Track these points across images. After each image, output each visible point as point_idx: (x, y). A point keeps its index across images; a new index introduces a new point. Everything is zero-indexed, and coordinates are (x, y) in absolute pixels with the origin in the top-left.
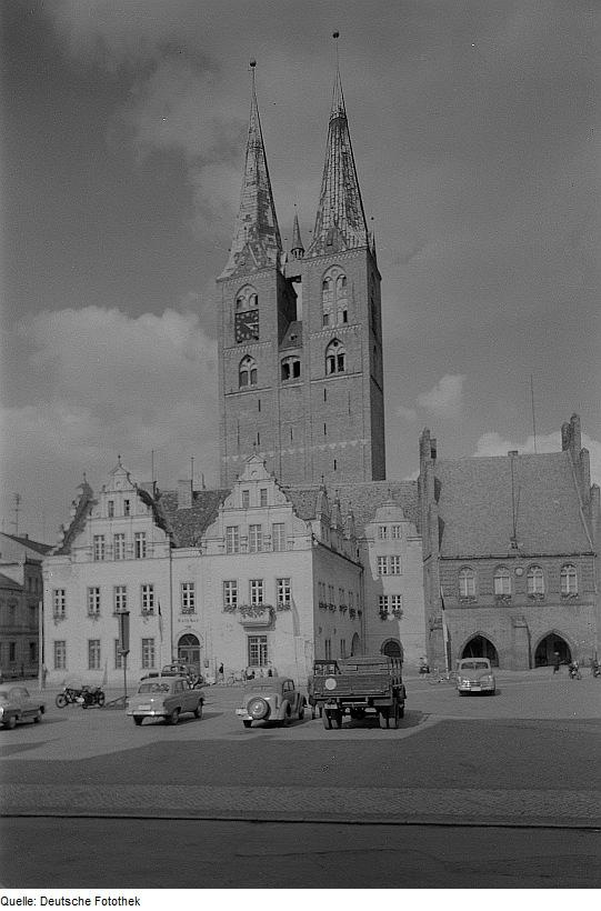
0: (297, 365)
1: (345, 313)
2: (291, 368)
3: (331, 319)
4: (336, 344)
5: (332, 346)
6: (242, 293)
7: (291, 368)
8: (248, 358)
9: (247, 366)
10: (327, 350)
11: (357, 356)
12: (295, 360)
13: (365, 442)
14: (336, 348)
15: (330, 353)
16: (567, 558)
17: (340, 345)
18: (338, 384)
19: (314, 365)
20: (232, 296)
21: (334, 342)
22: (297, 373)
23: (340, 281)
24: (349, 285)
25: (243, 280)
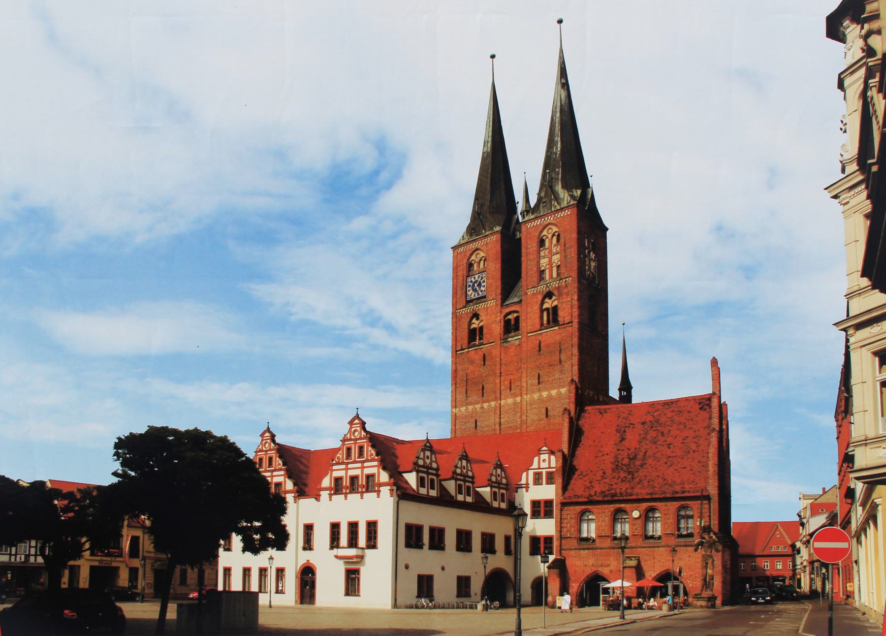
0: (517, 319)
1: (558, 267)
2: (513, 323)
3: (547, 276)
4: (550, 298)
5: (547, 300)
8: (476, 316)
9: (476, 324)
10: (542, 303)
11: (569, 308)
12: (515, 315)
13: (563, 390)
14: (550, 301)
15: (545, 306)
16: (702, 504)
17: (554, 298)
18: (552, 334)
19: (530, 318)
20: (465, 261)
21: (549, 295)
22: (517, 328)
23: (555, 239)
24: (562, 241)
25: (473, 246)
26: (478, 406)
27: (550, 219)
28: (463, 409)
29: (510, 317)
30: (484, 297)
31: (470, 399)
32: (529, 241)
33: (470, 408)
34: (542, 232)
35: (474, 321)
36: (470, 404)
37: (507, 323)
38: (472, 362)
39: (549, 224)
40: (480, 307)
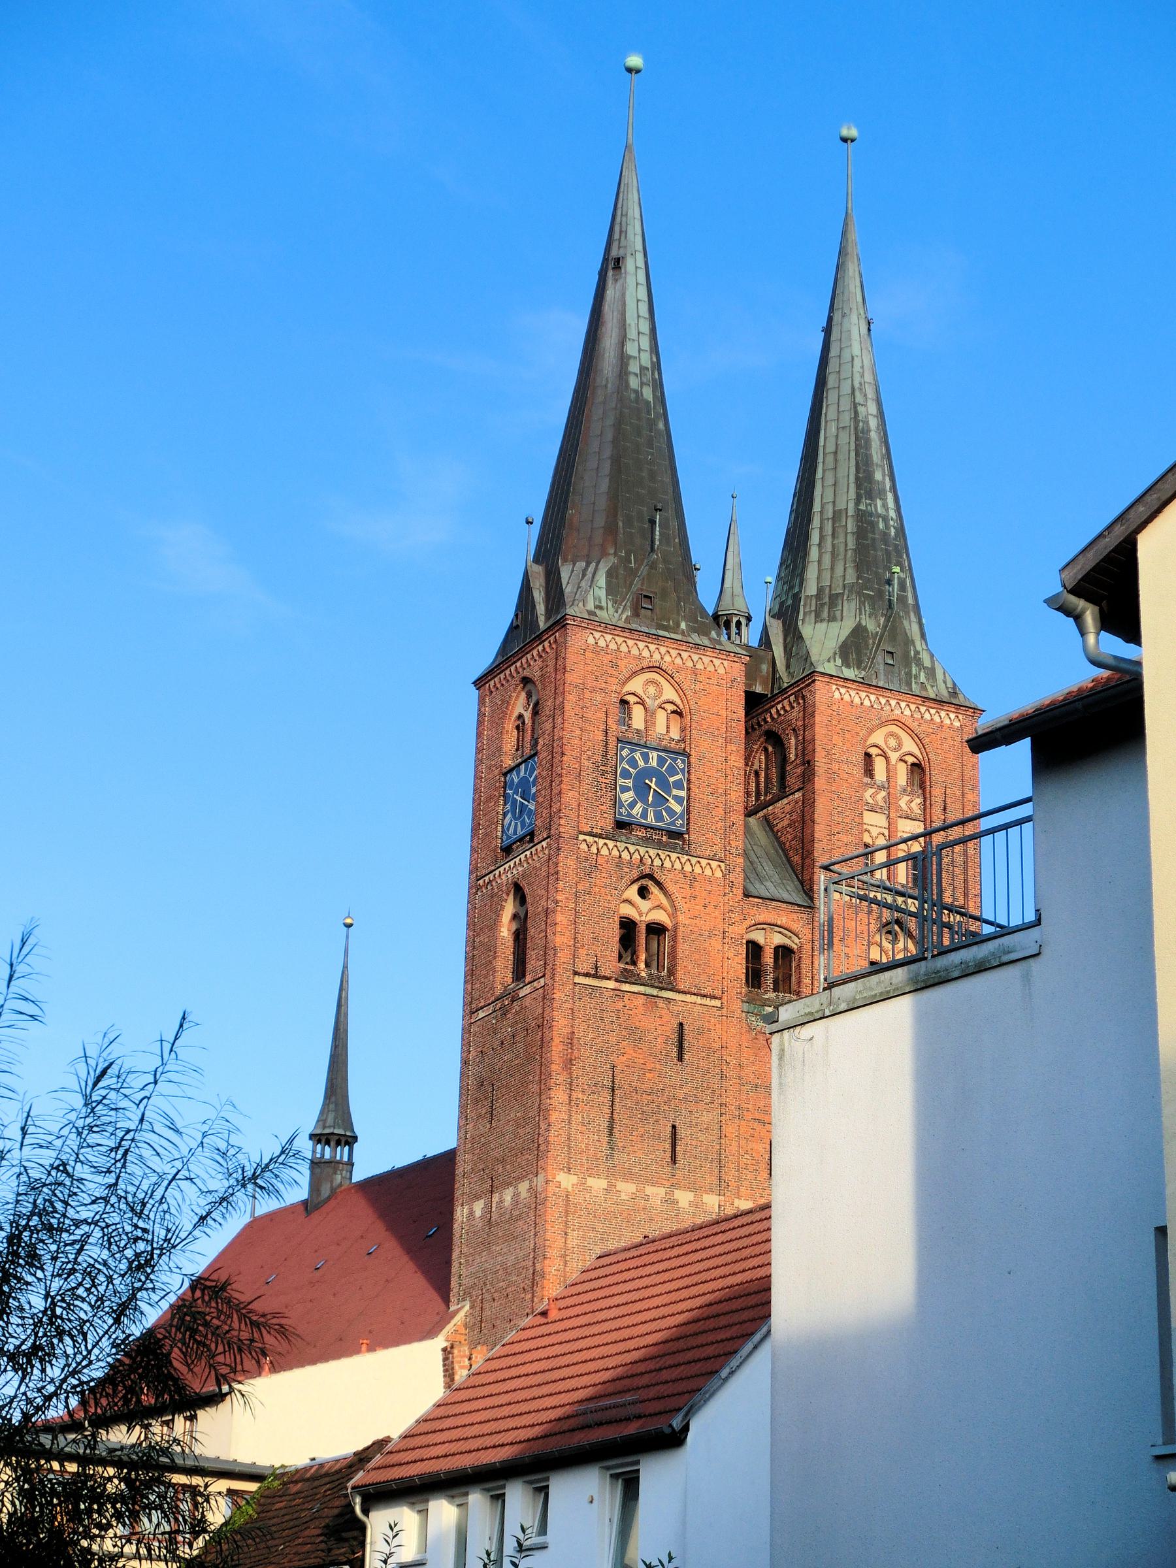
2: (768, 958)
6: (636, 685)
7: (768, 958)
12: (778, 939)
24: (937, 792)
26: (656, 1192)
27: (905, 709)
28: (598, 1184)
29: (759, 937)
30: (677, 835)
31: (621, 1158)
32: (836, 739)
33: (626, 1189)
34: (871, 731)
35: (632, 892)
36: (628, 1176)
37: (754, 950)
38: (634, 1034)
39: (897, 722)
40: (669, 862)
